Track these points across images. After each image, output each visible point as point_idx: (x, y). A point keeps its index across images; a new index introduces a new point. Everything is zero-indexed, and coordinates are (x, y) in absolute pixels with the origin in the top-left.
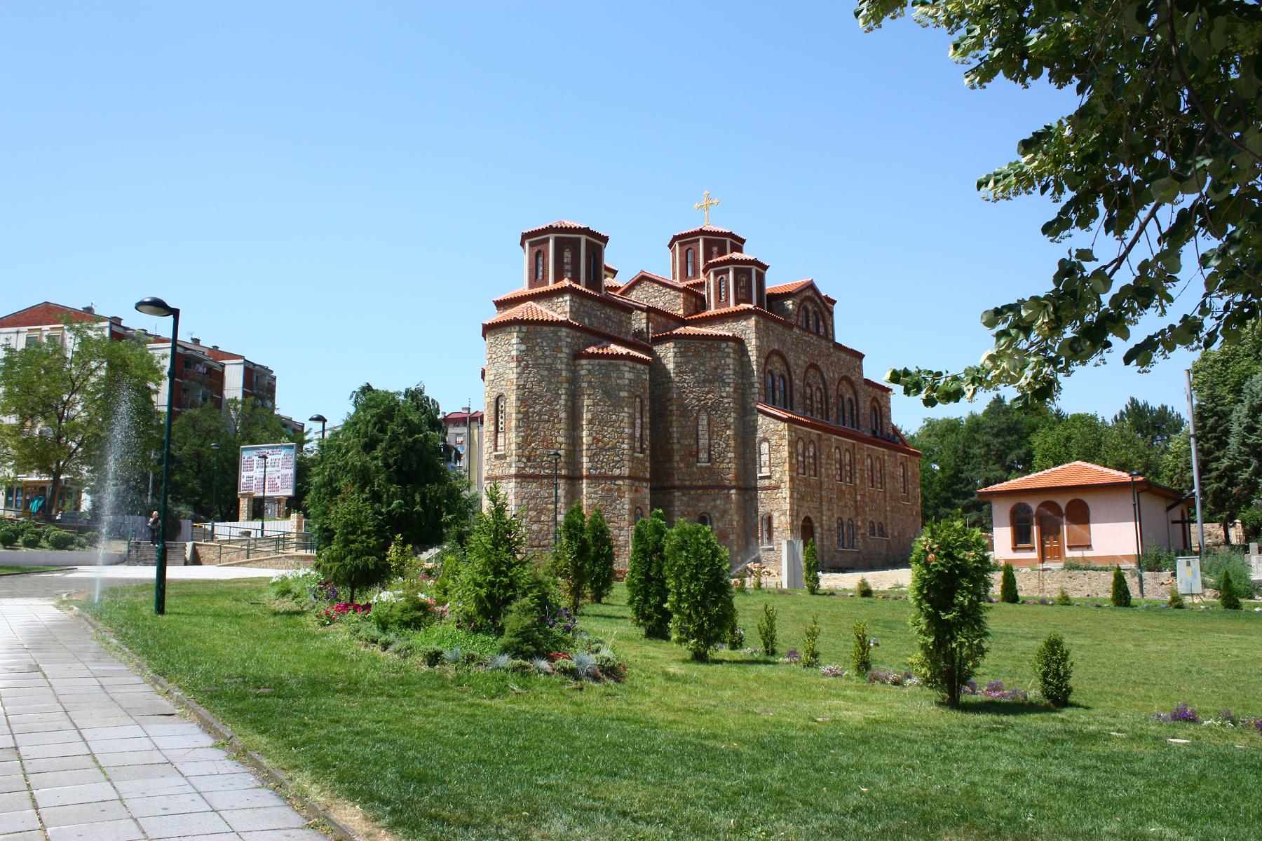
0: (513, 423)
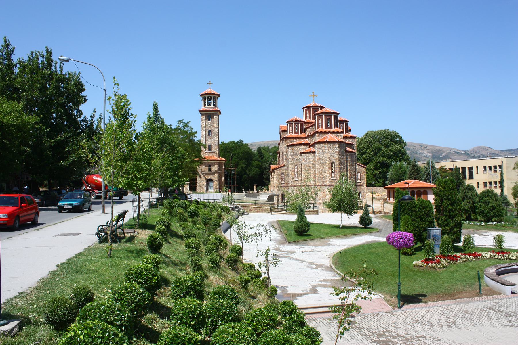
0: (338, 170)
